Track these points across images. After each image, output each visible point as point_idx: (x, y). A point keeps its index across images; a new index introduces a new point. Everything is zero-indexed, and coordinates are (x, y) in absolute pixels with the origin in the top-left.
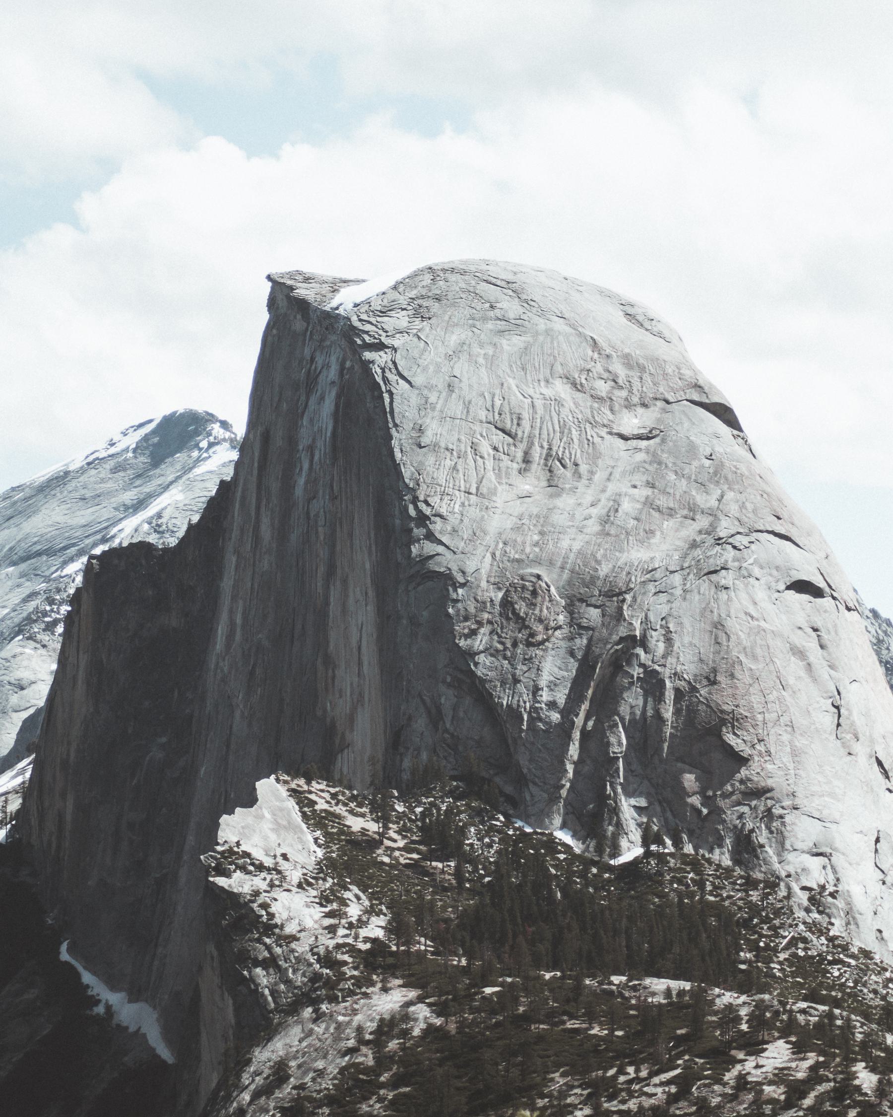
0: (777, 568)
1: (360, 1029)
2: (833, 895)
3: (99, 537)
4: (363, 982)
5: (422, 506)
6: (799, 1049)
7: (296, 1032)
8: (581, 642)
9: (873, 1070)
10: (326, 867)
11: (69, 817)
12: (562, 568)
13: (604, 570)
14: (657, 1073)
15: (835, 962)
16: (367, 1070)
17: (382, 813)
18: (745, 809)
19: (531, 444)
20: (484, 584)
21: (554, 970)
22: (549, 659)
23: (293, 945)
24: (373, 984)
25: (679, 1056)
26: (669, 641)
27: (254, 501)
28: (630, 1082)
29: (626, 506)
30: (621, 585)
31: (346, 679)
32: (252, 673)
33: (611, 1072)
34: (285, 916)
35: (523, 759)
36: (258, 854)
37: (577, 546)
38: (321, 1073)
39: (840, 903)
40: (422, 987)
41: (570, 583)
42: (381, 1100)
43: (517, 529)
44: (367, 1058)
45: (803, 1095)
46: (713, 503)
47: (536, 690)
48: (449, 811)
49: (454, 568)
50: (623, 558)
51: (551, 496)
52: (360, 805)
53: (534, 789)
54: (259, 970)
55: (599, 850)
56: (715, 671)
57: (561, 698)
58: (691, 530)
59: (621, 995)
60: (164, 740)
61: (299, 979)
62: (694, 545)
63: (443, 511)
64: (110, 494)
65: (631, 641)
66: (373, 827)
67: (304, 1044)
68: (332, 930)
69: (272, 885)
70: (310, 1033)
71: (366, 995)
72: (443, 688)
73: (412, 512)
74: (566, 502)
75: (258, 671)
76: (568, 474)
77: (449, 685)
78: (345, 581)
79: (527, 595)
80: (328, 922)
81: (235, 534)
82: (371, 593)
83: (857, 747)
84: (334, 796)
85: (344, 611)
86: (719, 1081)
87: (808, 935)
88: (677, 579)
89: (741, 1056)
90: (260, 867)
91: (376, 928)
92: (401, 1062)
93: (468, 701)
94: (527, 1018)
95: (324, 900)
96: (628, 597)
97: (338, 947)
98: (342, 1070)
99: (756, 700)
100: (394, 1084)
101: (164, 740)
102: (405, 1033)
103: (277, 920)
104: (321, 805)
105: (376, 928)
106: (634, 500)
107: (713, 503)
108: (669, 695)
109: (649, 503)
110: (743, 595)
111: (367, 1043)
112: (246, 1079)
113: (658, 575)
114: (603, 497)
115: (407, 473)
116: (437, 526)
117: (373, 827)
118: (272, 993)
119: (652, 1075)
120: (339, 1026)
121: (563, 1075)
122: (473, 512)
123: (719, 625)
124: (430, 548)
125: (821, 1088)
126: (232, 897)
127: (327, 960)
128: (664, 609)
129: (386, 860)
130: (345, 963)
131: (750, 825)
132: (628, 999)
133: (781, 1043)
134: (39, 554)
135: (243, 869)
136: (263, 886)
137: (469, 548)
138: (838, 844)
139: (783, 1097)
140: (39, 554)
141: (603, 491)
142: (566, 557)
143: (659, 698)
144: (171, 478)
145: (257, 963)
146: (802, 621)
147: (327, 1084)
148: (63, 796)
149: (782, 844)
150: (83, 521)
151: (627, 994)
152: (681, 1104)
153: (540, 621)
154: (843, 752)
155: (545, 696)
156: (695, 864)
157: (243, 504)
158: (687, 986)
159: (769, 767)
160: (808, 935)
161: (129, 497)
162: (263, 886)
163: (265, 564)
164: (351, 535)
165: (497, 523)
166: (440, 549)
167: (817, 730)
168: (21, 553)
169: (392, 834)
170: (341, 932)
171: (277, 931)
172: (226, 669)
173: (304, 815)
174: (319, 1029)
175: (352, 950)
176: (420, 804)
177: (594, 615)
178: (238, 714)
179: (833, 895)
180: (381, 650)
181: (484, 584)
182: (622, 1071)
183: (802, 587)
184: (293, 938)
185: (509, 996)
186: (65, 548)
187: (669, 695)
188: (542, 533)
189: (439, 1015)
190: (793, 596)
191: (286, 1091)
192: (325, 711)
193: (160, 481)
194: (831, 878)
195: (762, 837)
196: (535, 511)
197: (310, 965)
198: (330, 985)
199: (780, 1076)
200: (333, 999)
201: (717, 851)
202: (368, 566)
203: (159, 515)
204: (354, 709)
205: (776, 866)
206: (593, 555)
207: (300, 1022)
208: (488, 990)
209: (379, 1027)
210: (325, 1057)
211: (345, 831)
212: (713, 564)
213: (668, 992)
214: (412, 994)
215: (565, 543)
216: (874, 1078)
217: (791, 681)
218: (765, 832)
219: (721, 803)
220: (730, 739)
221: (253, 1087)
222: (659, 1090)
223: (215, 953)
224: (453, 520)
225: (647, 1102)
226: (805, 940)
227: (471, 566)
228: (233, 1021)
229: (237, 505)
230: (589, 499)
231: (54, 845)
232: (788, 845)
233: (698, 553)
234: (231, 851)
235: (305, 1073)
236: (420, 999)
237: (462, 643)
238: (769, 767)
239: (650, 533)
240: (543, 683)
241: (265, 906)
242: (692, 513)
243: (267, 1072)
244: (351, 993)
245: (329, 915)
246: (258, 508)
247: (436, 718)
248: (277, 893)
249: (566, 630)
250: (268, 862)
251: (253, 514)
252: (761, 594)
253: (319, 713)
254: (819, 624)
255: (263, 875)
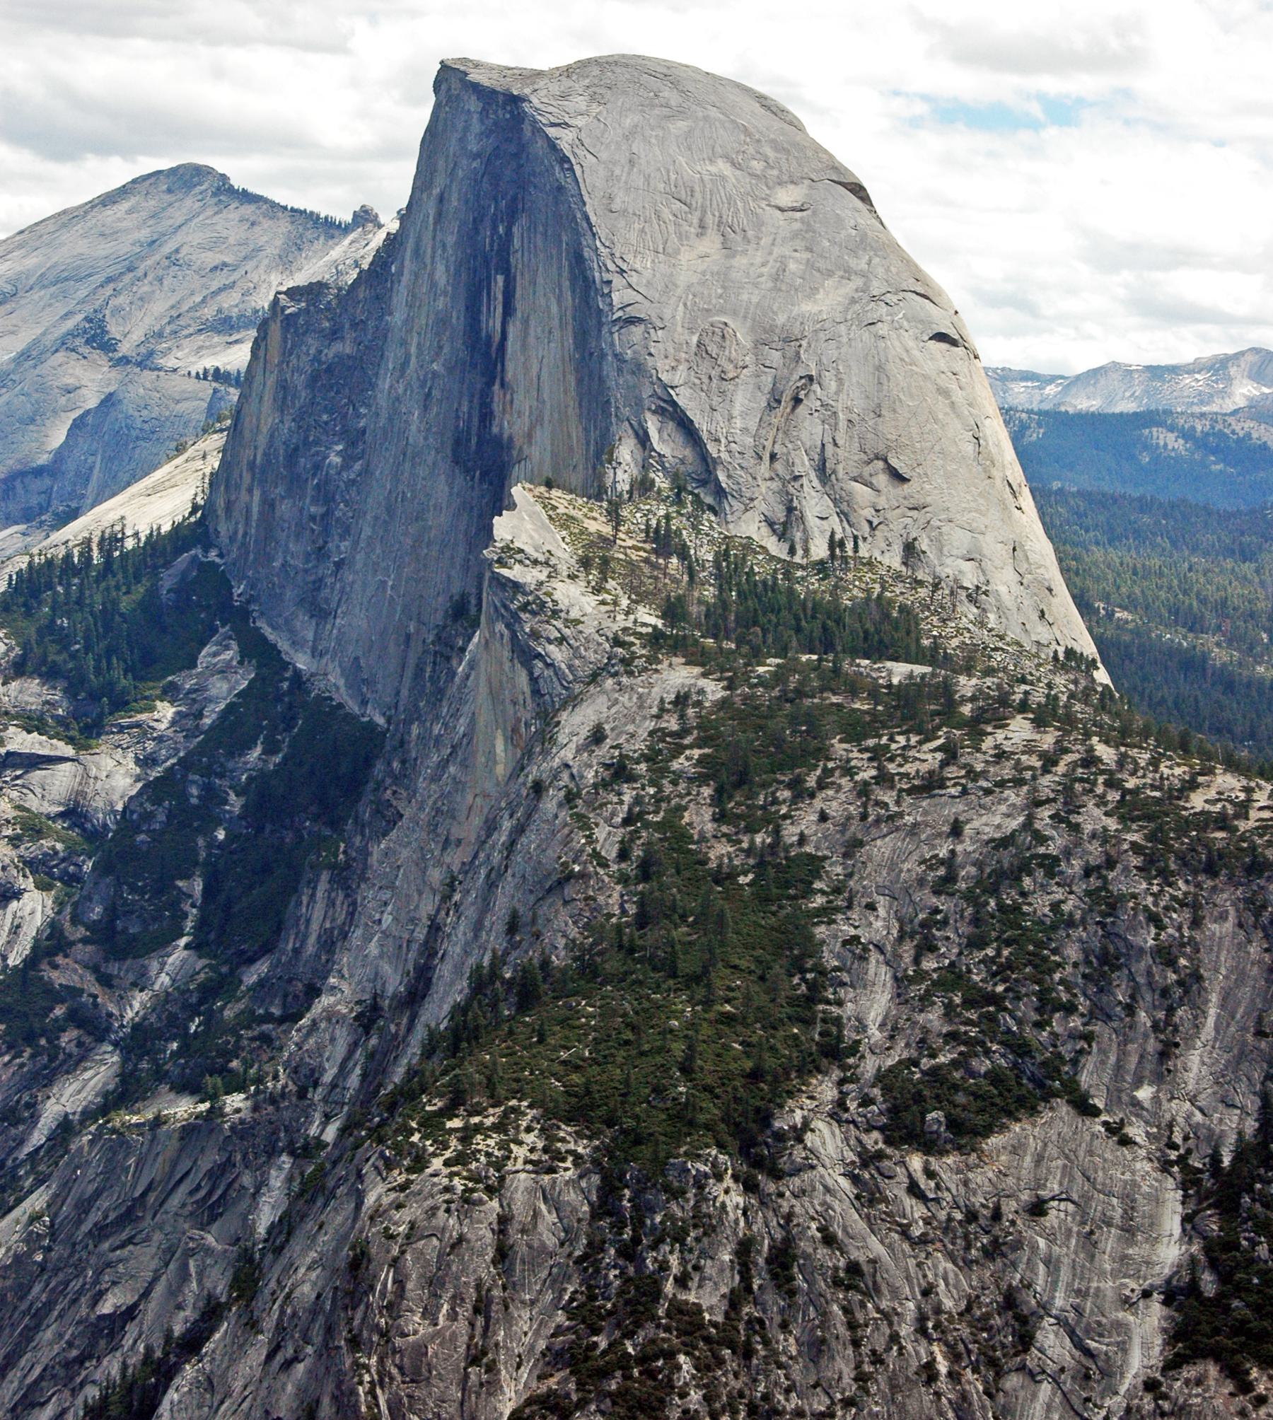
0: (922, 322)
1: (662, 700)
2: (986, 593)
3: (119, 268)
4: (652, 659)
5: (620, 262)
6: (1040, 723)
7: (602, 700)
8: (767, 380)
9: (1107, 743)
10: (585, 563)
11: (255, 509)
12: (745, 317)
13: (781, 319)
14: (928, 740)
15: (996, 649)
16: (672, 734)
17: (614, 516)
18: (909, 521)
19: (704, 212)
20: (679, 329)
21: (811, 652)
22: (740, 393)
23: (580, 627)
24: (660, 662)
25: (939, 728)
26: (840, 381)
27: (429, 251)
28: (904, 748)
29: (792, 266)
30: (796, 332)
31: (523, 401)
32: (428, 395)
33: (884, 740)
34: (566, 602)
35: (722, 477)
36: (529, 550)
37: (755, 299)
38: (633, 736)
39: (991, 600)
40: (703, 665)
41: (752, 329)
42: (687, 759)
43: (703, 283)
44: (672, 724)
45: (1055, 763)
46: (863, 266)
47: (731, 418)
48: (668, 517)
49: (653, 315)
50: (796, 311)
51: (727, 257)
52: (591, 510)
53: (733, 502)
54: (552, 648)
55: (792, 551)
56: (879, 406)
57: (753, 425)
58: (849, 288)
59: (868, 675)
60: (340, 447)
61: (591, 656)
62: (853, 301)
63: (638, 266)
64: (127, 230)
65: (811, 378)
66: (607, 530)
67: (613, 710)
68: (611, 615)
69: (549, 576)
70: (616, 702)
71: (657, 671)
72: (648, 415)
73: (611, 266)
74: (740, 261)
75: (436, 393)
76: (739, 238)
77: (654, 412)
78: (526, 322)
79: (717, 339)
80: (604, 608)
81: (405, 279)
82: (557, 333)
83: (994, 472)
84: (570, 502)
85: (524, 346)
86: (979, 750)
87: (970, 626)
88: (842, 328)
89: (989, 729)
90: (536, 562)
91: (648, 617)
92: (699, 727)
93: (671, 425)
94: (800, 693)
95: (598, 590)
96: (804, 343)
97: (625, 630)
98: (651, 734)
99: (914, 430)
100: (697, 744)
101: (340, 447)
102: (699, 704)
103: (561, 606)
104: (561, 510)
105: (648, 617)
106: (797, 261)
107: (863, 266)
108: (842, 424)
109: (810, 264)
110: (897, 344)
111: (668, 711)
112: (562, 739)
113: (827, 325)
114: (771, 259)
115: (602, 231)
116: (634, 279)
117: (607, 530)
118: (570, 667)
119: (920, 743)
120: (640, 697)
121: (841, 741)
122: (663, 268)
123: (879, 368)
124: (630, 296)
125: (1069, 758)
126: (517, 587)
127: (617, 642)
128: (833, 354)
129: (622, 556)
130: (633, 644)
131: (914, 535)
132: (876, 679)
133: (1019, 717)
134: (66, 279)
135: (520, 562)
136: (543, 577)
137: (664, 299)
138: (986, 552)
139: (1038, 764)
140: (66, 279)
141: (770, 253)
142: (747, 309)
143: (835, 427)
144: (180, 220)
145: (550, 641)
146: (943, 365)
147: (640, 746)
148: (250, 491)
149: (941, 551)
150: (104, 253)
151: (874, 675)
152: (952, 768)
153: (730, 361)
154: (983, 476)
155: (738, 423)
156: (870, 564)
157: (417, 253)
158: (927, 669)
159: (927, 487)
160: (970, 626)
161: (144, 234)
162: (543, 577)
163: (440, 304)
164: (534, 283)
165: (683, 279)
166: (639, 298)
167: (964, 458)
168: (51, 278)
169: (621, 535)
170: (620, 617)
171: (563, 615)
172: (400, 391)
173: (550, 517)
174: (624, 699)
175: (635, 634)
176: (639, 510)
177: (775, 357)
178: (413, 428)
179: (986, 593)
180: (579, 381)
181: (679, 329)
182: (892, 739)
183: (941, 337)
184: (577, 622)
185: (779, 676)
186: (90, 275)
187: (842, 424)
188: (723, 287)
189: (724, 688)
190: (933, 344)
191: (604, 752)
192: (501, 427)
193: (170, 222)
194: (982, 579)
195: (924, 544)
196: (716, 269)
197: (599, 644)
198: (623, 661)
199: (1029, 748)
200: (630, 674)
201: (887, 555)
202: (554, 309)
203: (177, 251)
204: (532, 428)
205: (938, 569)
206: (770, 307)
207: (603, 692)
208: (761, 669)
209: (677, 697)
210: (633, 722)
211: (584, 531)
212: (871, 317)
213: (910, 676)
214: (697, 670)
215: (745, 297)
216: (1112, 751)
217: (941, 416)
218: (926, 541)
219: (890, 515)
220: (893, 462)
221: (573, 746)
222: (929, 756)
223: (506, 632)
224: (647, 274)
225: (924, 768)
226: (969, 631)
227: (667, 314)
228: (527, 690)
229: (408, 254)
230: (758, 260)
231: (241, 532)
232: (945, 550)
233: (857, 307)
234: (508, 547)
235: (619, 735)
236: (704, 675)
237: (664, 377)
238: (927, 487)
239: (814, 290)
240: (736, 413)
241: (549, 594)
242: (848, 273)
243: (584, 732)
244: (645, 669)
245: (603, 603)
246: (433, 257)
247: (643, 439)
248: (555, 583)
249: (752, 368)
250: (541, 558)
251: (428, 261)
252: (911, 344)
253: (495, 430)
254: (956, 370)
255: (539, 567)
